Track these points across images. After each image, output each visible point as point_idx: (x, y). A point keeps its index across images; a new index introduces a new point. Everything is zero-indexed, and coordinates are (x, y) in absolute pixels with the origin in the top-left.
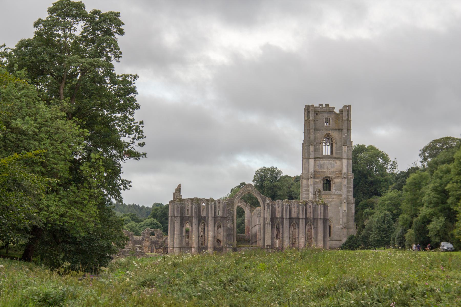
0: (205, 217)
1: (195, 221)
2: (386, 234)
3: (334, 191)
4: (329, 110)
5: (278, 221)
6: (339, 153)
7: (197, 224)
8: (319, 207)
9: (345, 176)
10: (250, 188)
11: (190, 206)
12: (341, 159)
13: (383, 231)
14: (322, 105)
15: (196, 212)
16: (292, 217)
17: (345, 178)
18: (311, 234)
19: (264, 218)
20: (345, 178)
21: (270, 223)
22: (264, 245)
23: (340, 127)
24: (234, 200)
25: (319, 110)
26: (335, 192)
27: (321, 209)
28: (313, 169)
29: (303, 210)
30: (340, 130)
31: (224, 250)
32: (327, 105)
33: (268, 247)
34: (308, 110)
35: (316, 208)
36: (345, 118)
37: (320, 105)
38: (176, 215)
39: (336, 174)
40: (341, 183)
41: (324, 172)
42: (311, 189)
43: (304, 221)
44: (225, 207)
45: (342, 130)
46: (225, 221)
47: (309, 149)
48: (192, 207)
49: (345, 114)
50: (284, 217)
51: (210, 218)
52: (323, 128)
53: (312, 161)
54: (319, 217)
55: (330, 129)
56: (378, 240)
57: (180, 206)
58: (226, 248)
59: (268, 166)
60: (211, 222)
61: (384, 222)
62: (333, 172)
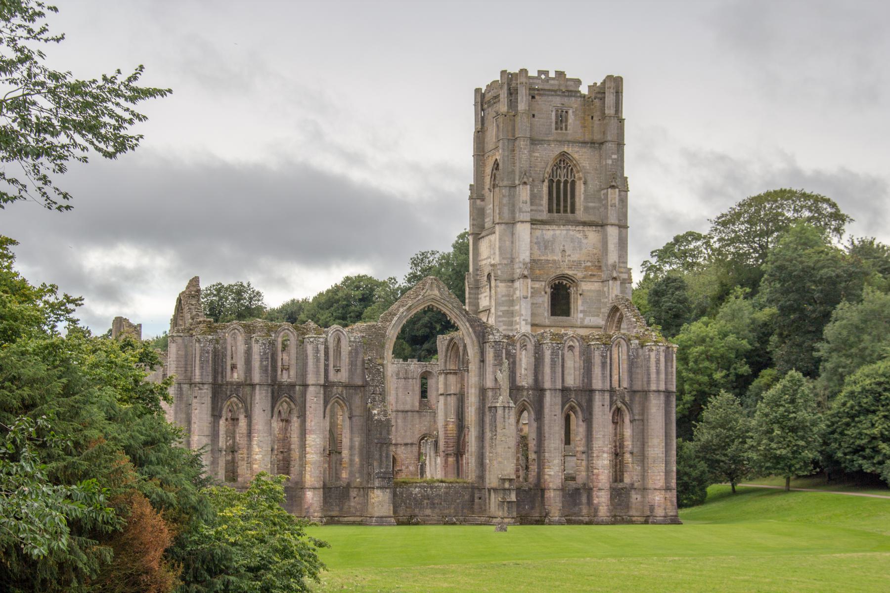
0: (292, 386)
1: (260, 400)
2: (802, 438)
3: (581, 315)
4: (564, 87)
5: (525, 396)
6: (594, 208)
7: (269, 408)
8: (653, 355)
9: (615, 275)
10: (436, 292)
11: (241, 348)
12: (601, 225)
13: (793, 430)
14: (546, 73)
15: (264, 370)
16: (566, 385)
17: (615, 279)
18: (622, 439)
19: (483, 391)
20: (615, 279)
21: (512, 405)
22: (481, 477)
23: (597, 137)
24: (385, 328)
25: (540, 87)
26: (583, 319)
27: (658, 361)
28: (528, 253)
29: (604, 364)
30: (596, 145)
31: (353, 493)
32: (560, 74)
33: (507, 485)
34: (509, 85)
35: (637, 356)
36: (610, 111)
37: (540, 72)
38: (197, 378)
39: (586, 268)
40: (600, 293)
41: (554, 262)
42: (524, 309)
43: (607, 396)
44: (357, 353)
45: (602, 143)
46: (357, 400)
47: (512, 197)
48: (248, 353)
49: (610, 99)
50: (547, 385)
51: (311, 389)
52: (551, 138)
53: (523, 231)
54: (653, 387)
56: (778, 459)
57: (210, 348)
58: (365, 490)
59: (228, 281)
60: (314, 399)
61: (793, 401)
62: (579, 263)
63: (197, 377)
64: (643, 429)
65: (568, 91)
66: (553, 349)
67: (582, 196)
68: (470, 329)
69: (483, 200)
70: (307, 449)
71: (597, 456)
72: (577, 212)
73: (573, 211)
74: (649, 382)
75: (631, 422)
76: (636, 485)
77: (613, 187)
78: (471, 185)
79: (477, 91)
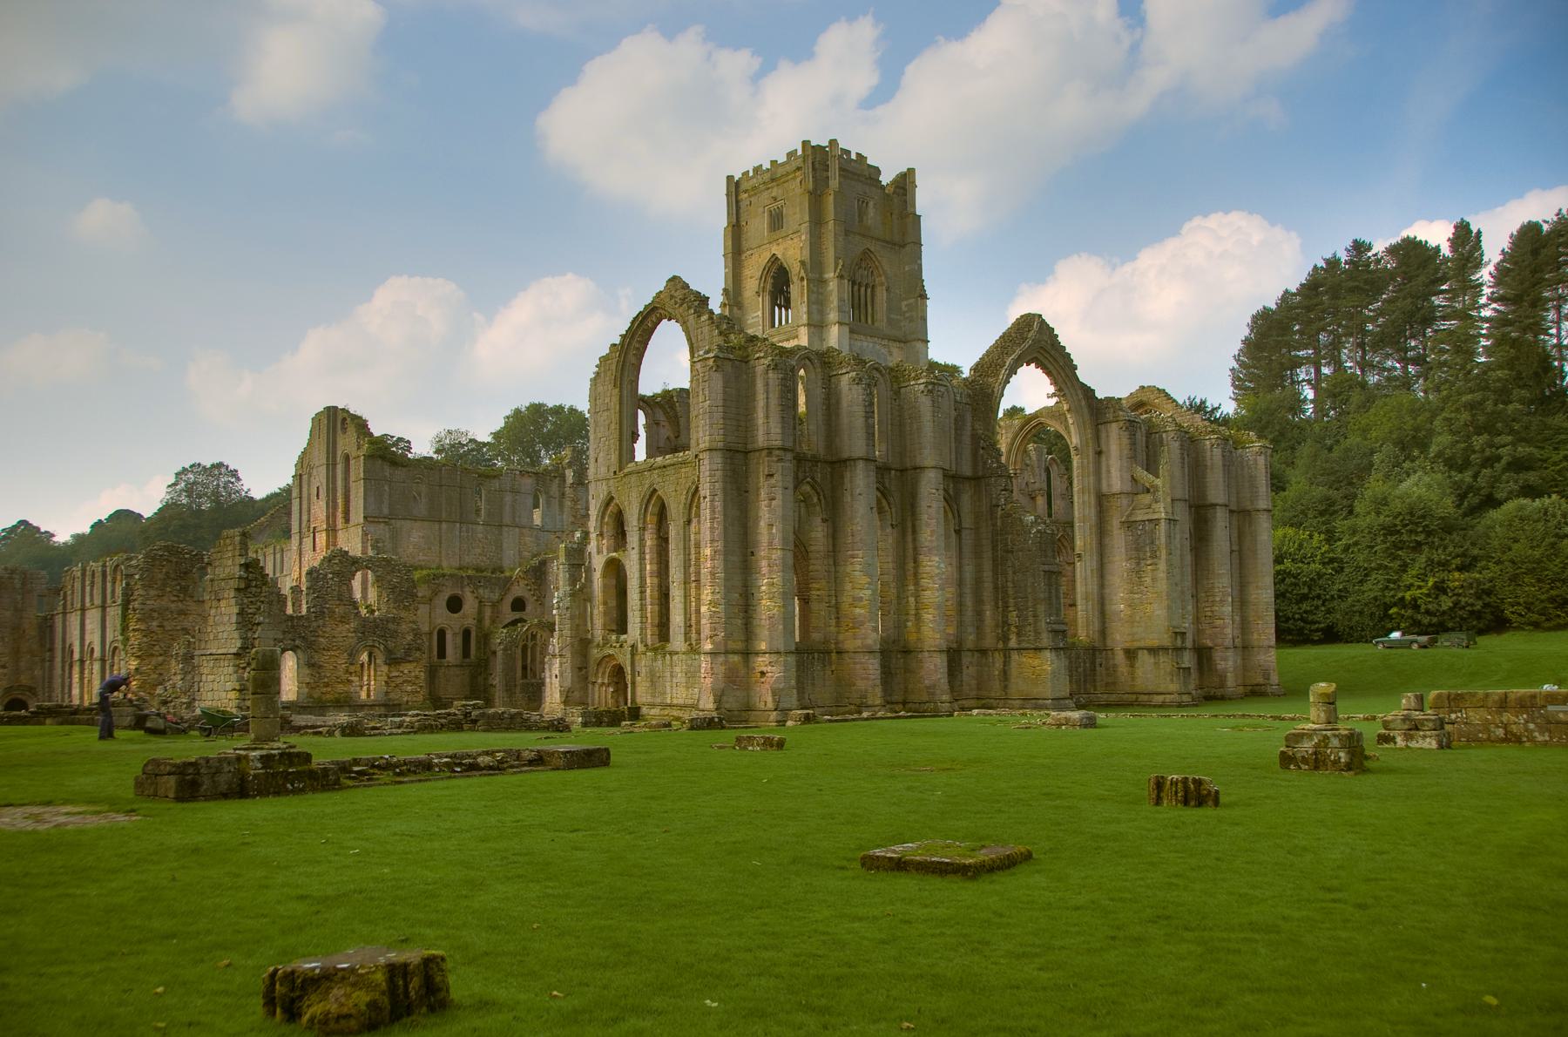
45: (903, 246)
70: (924, 582)
79: (730, 178)
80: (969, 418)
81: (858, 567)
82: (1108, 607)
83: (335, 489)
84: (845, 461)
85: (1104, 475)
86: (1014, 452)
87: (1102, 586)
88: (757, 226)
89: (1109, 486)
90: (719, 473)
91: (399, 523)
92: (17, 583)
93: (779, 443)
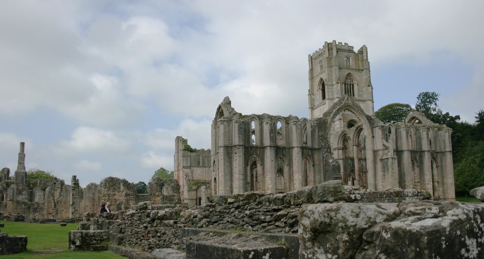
1: (269, 154)
14: (341, 43)
21: (396, 157)
23: (361, 68)
36: (365, 58)
45: (363, 70)
55: (351, 69)
63: (236, 142)
64: (442, 170)
65: (349, 50)
66: (407, 130)
67: (357, 90)
68: (367, 121)
69: (314, 95)
71: (428, 183)
72: (355, 96)
73: (353, 96)
74: (445, 147)
75: (437, 167)
76: (441, 197)
77: (369, 86)
78: (309, 90)
79: (309, 55)
80: (317, 130)
81: (268, 178)
82: (377, 187)
83: (179, 159)
84: (265, 147)
85: (375, 144)
86: (355, 138)
87: (375, 180)
88: (317, 69)
89: (376, 148)
90: (223, 153)
91: (193, 168)
92: (93, 187)
93: (238, 144)
